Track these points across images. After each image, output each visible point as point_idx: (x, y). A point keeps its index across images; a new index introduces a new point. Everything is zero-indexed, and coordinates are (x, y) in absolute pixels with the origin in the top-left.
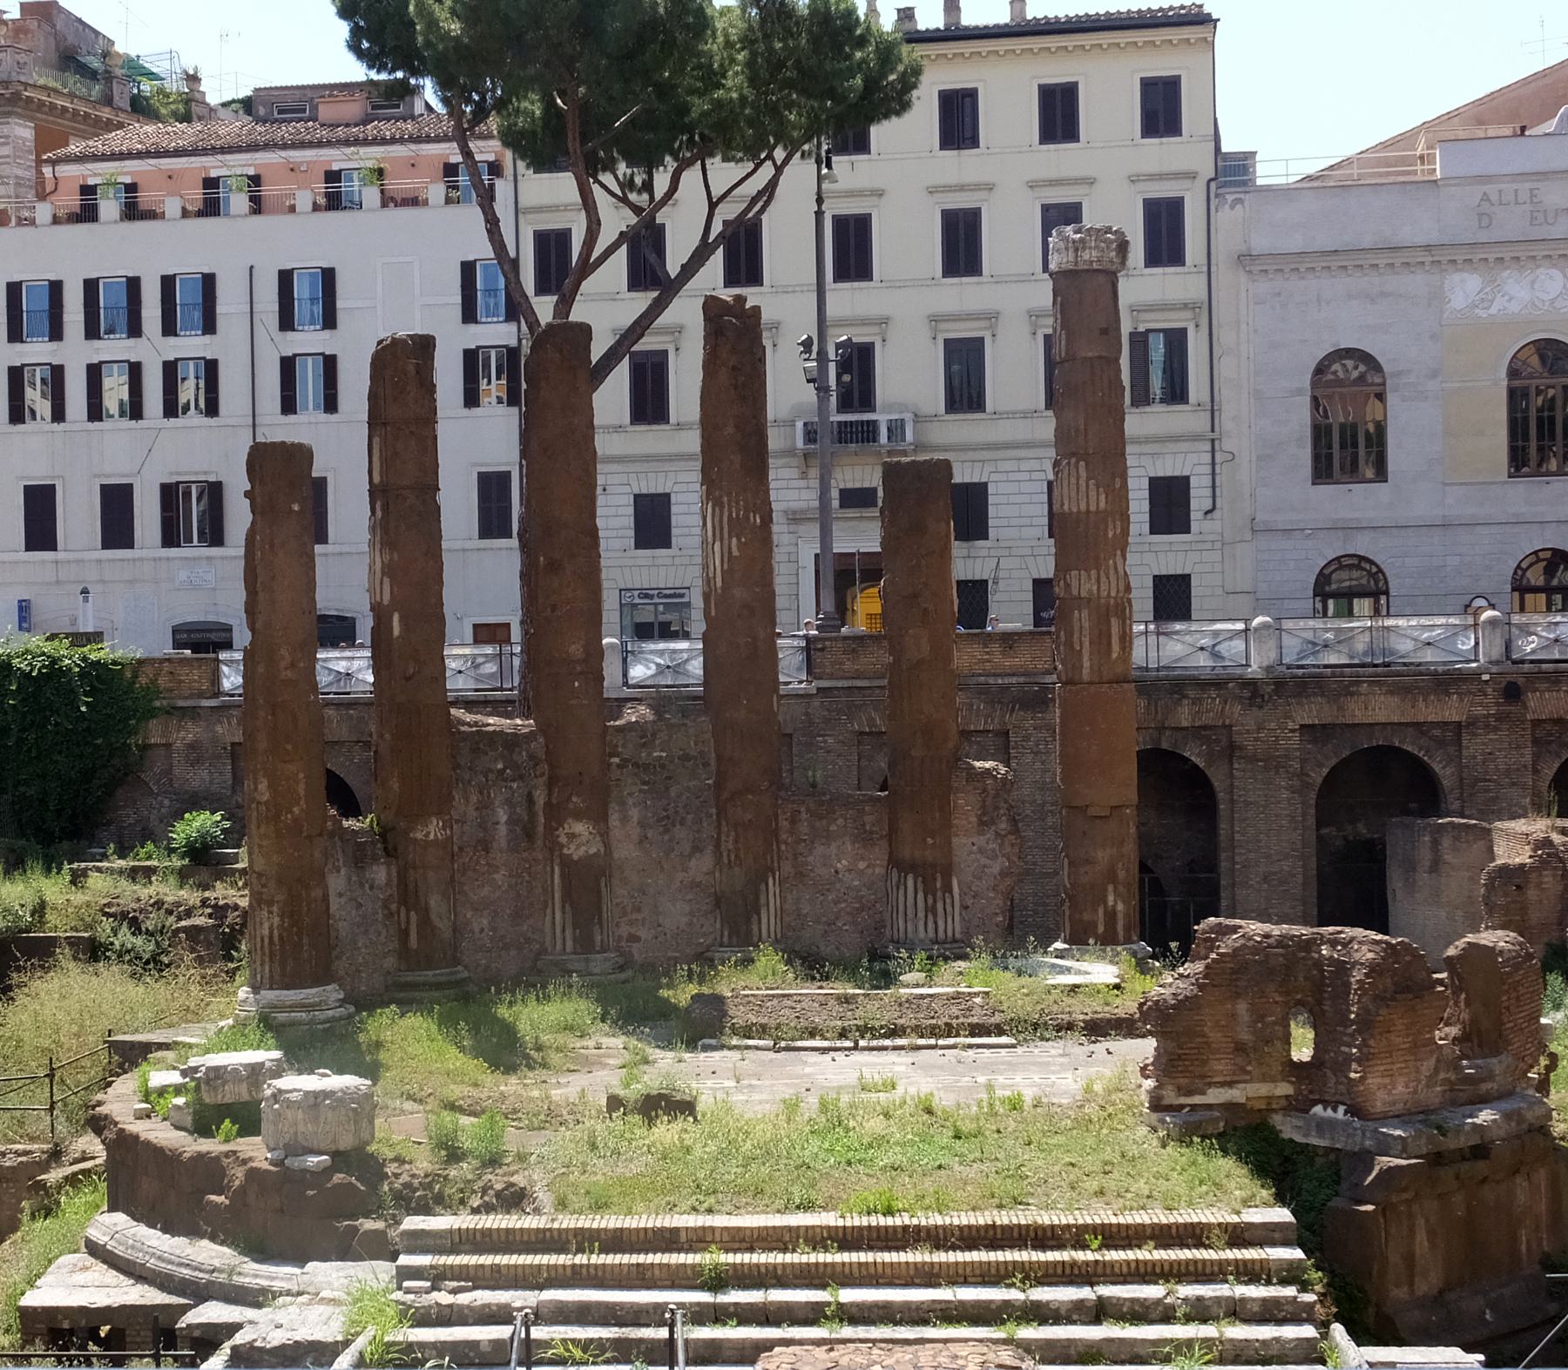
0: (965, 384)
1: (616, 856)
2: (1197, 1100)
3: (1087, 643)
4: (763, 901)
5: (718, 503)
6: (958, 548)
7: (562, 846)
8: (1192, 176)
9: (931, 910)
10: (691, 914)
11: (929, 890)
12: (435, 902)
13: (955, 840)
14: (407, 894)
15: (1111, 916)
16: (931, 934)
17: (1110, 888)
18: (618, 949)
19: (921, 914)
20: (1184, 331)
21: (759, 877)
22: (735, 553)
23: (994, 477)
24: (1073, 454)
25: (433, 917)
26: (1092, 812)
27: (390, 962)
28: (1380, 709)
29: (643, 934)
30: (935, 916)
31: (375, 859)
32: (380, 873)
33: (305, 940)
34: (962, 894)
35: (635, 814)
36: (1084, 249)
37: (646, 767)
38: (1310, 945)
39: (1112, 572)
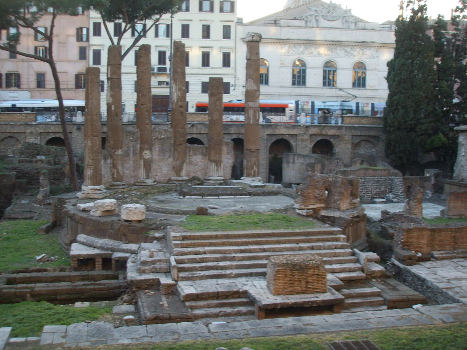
0: (226, 61)
3: (252, 116)
5: (176, 84)
6: (225, 95)
7: (143, 156)
8: (233, 21)
9: (217, 170)
10: (168, 170)
11: (217, 166)
12: (120, 168)
13: (223, 156)
14: (114, 166)
15: (255, 171)
18: (154, 178)
19: (215, 171)
20: (230, 53)
21: (183, 163)
23: (191, 80)
24: (250, 78)
27: (110, 180)
28: (283, 131)
29: (159, 174)
32: (109, 161)
34: (223, 167)
35: (157, 149)
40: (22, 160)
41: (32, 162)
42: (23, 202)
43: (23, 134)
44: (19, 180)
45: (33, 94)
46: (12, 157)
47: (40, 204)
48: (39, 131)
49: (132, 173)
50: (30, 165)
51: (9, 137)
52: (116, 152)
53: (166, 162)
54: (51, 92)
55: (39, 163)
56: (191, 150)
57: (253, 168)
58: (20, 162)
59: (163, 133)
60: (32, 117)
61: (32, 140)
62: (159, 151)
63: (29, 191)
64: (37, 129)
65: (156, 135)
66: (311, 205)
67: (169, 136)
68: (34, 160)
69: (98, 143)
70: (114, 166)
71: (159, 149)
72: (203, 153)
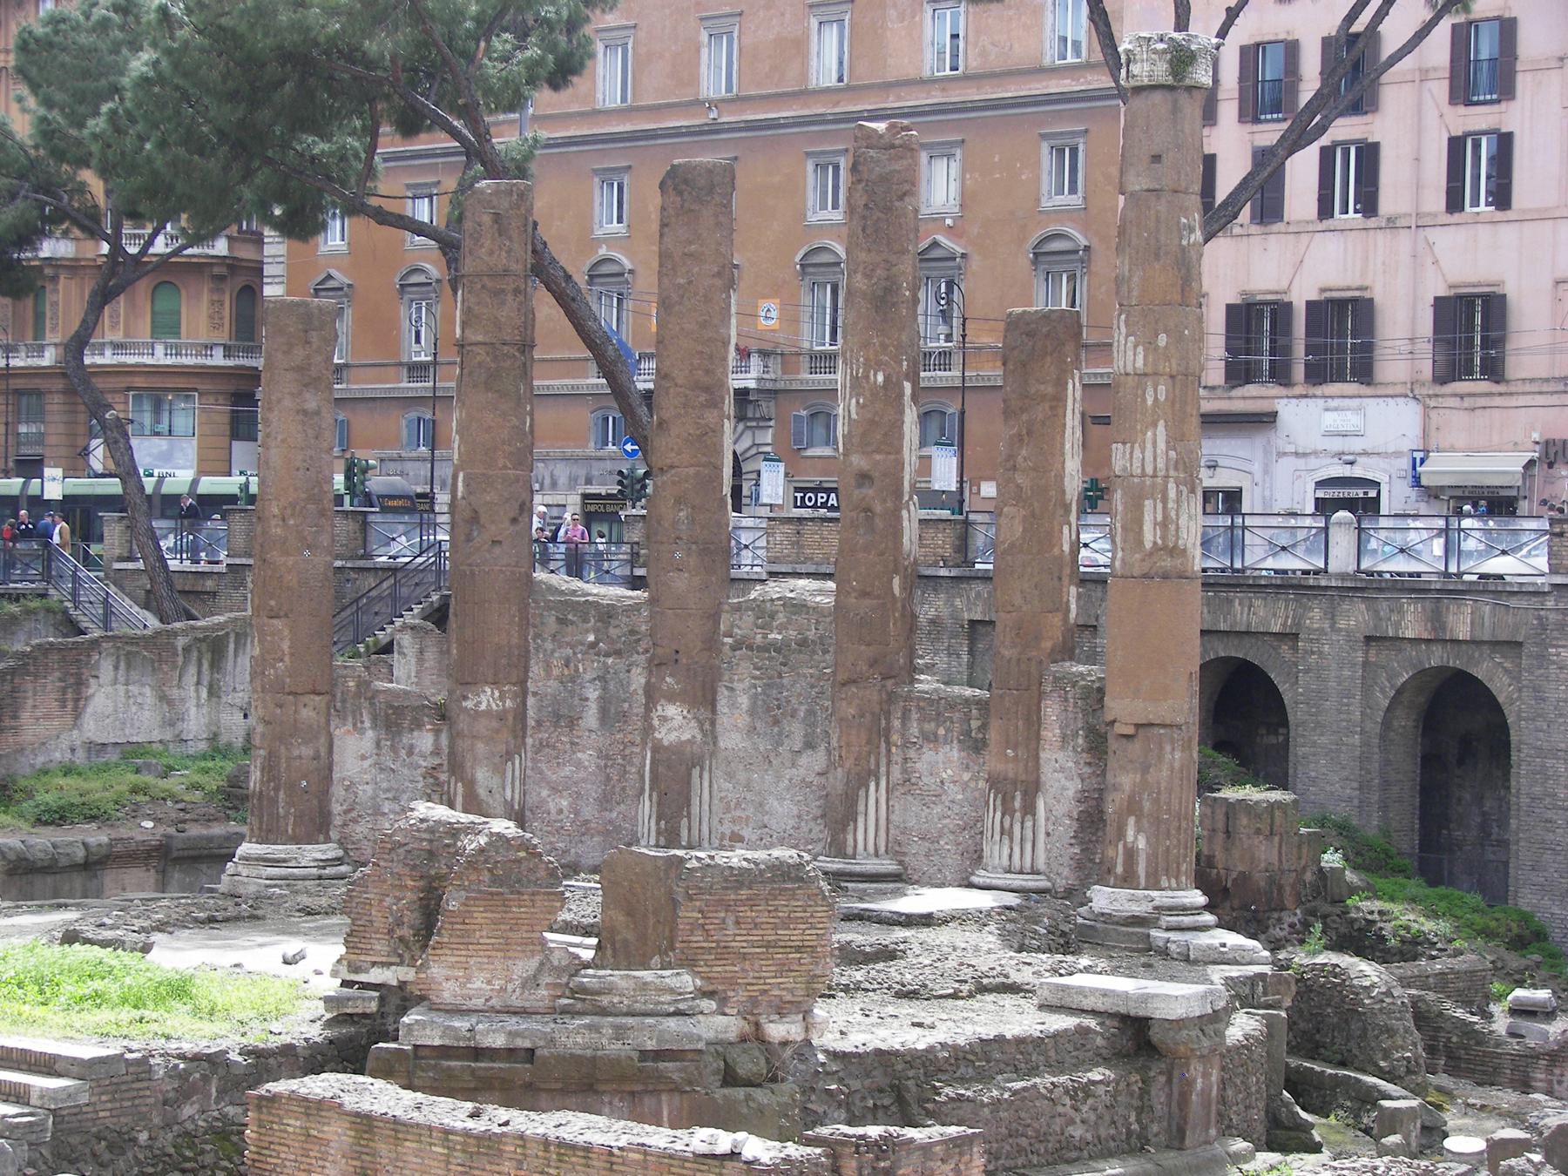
1: (722, 744)
2: (362, 978)
4: (861, 808)
11: (1007, 810)
13: (1042, 755)
15: (1131, 854)
16: (1005, 862)
17: (1132, 820)
19: (997, 837)
21: (862, 779)
22: (854, 416)
25: (482, 792)
26: (1120, 729)
30: (1011, 840)
31: (417, 725)
32: (424, 741)
33: (282, 795)
35: (744, 701)
36: (1135, 61)
37: (765, 648)
38: (454, 831)
39: (1149, 446)
45: (1433, 414)
49: (588, 812)
52: (465, 698)
53: (788, 773)
54: (1522, 400)
56: (914, 715)
57: (1121, 834)
59: (781, 618)
62: (752, 712)
64: (958, 602)
65: (745, 625)
66: (374, 964)
67: (811, 634)
69: (285, 646)
70: (456, 766)
71: (754, 698)
72: (968, 733)
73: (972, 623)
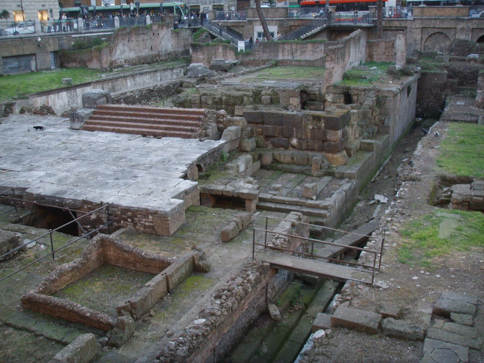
40: (453, 58)
41: (464, 60)
42: (458, 103)
43: (454, 30)
44: (450, 80)
46: (441, 55)
47: (478, 107)
48: (471, 27)
50: (462, 64)
51: (438, 33)
55: (472, 63)
58: (450, 60)
60: (464, 11)
61: (462, 37)
63: (462, 92)
64: (469, 24)
68: (467, 58)
73: (473, 29)
